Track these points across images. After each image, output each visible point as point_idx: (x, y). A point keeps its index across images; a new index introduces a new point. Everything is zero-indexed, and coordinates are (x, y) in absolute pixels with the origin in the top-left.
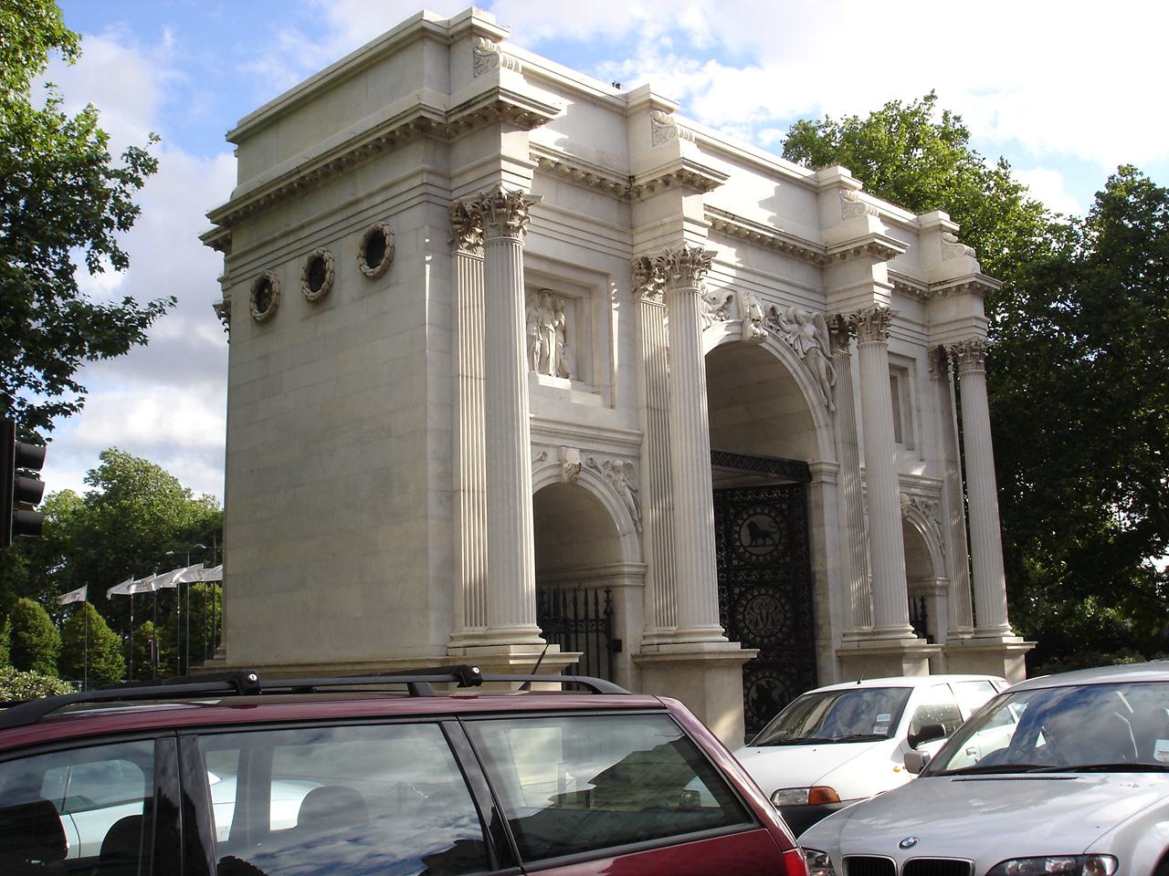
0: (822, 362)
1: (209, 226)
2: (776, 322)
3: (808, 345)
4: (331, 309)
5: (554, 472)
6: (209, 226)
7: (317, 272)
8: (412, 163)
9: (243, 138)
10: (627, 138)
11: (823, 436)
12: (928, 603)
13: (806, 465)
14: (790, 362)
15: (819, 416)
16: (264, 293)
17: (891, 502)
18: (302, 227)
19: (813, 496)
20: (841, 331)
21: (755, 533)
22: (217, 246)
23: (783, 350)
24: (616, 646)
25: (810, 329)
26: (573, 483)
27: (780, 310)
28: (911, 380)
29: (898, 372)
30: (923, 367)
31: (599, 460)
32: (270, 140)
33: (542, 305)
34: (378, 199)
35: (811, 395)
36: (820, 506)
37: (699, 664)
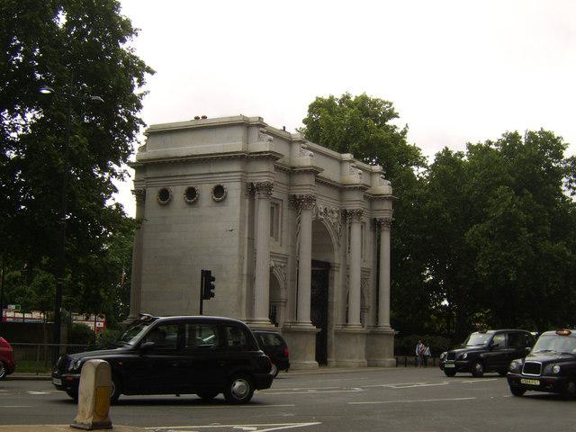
4: (198, 207)
7: (191, 194)
8: (236, 167)
10: (290, 150)
11: (336, 254)
13: (329, 263)
14: (329, 227)
15: (336, 246)
16: (165, 195)
18: (185, 176)
25: (336, 215)
30: (368, 225)
34: (221, 175)
35: (334, 239)
36: (333, 278)
37: (305, 332)
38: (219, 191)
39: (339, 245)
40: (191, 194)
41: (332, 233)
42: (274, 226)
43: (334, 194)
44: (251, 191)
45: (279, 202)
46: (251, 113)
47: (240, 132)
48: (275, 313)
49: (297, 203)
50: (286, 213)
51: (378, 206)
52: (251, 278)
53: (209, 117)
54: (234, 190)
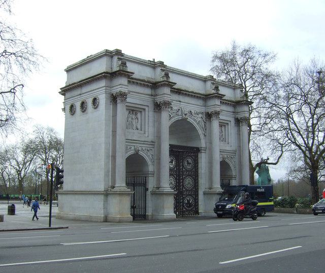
0: (203, 124)
1: (60, 91)
2: (191, 114)
3: (199, 119)
4: (87, 113)
5: (134, 151)
6: (60, 91)
8: (103, 83)
9: (69, 70)
10: (155, 74)
12: (231, 181)
14: (195, 124)
15: (202, 136)
17: (217, 158)
19: (199, 155)
20: (209, 116)
21: (188, 163)
22: (62, 94)
23: (192, 120)
24: (147, 190)
25: (200, 115)
26: (137, 153)
27: (193, 111)
28: (229, 126)
29: (222, 125)
31: (144, 148)
32: (74, 73)
33: (133, 113)
35: (200, 132)
38: (95, 101)
39: (205, 136)
40: (83, 105)
41: (197, 127)
42: (143, 124)
43: (200, 102)
44: (114, 99)
45: (147, 108)
46: (112, 48)
47: (105, 60)
48: (146, 182)
49: (158, 107)
50: (150, 114)
51: (240, 109)
52: (114, 157)
53: (93, 54)
54: (103, 99)
